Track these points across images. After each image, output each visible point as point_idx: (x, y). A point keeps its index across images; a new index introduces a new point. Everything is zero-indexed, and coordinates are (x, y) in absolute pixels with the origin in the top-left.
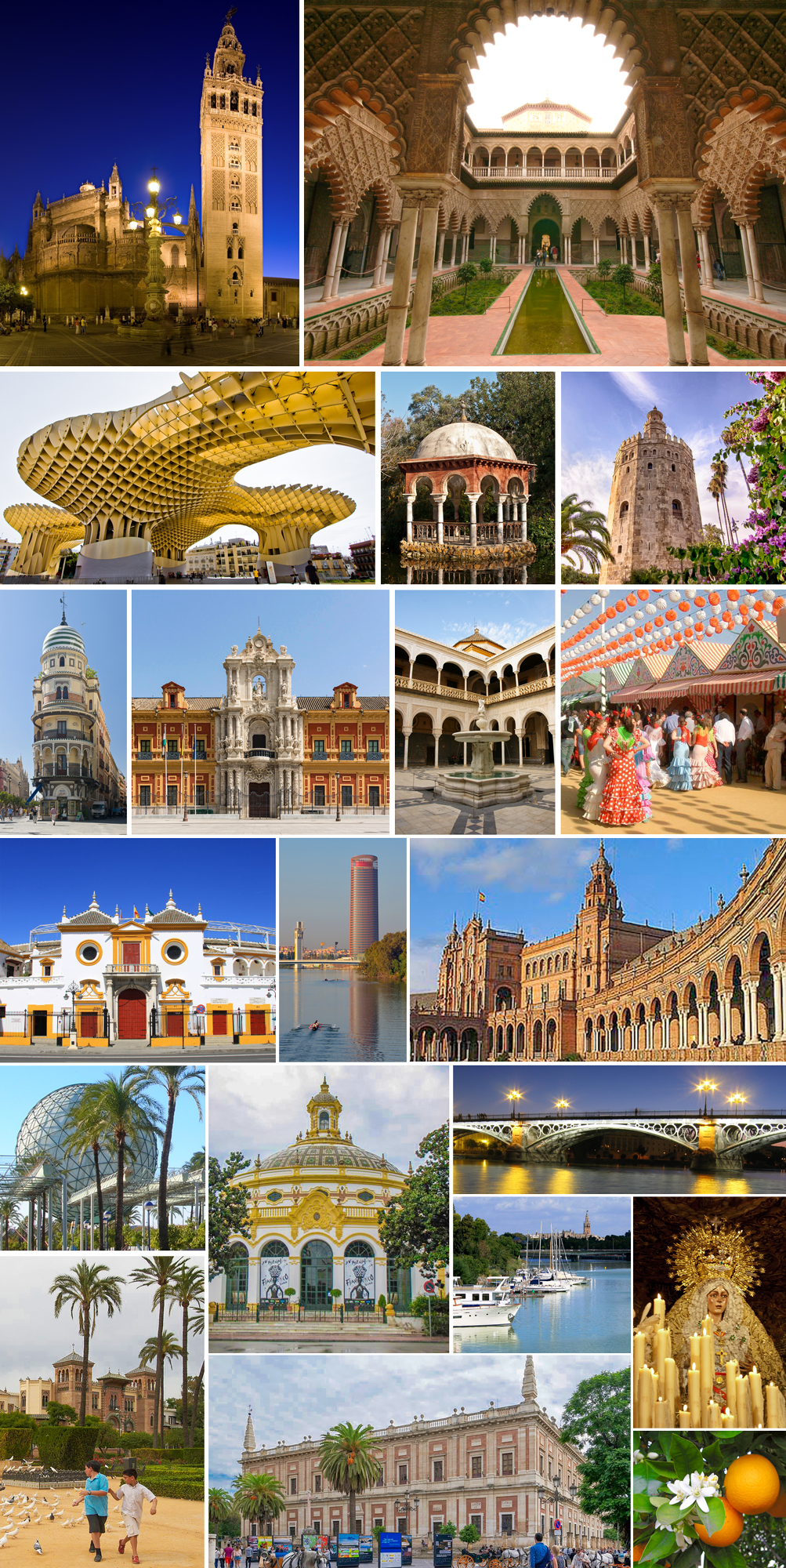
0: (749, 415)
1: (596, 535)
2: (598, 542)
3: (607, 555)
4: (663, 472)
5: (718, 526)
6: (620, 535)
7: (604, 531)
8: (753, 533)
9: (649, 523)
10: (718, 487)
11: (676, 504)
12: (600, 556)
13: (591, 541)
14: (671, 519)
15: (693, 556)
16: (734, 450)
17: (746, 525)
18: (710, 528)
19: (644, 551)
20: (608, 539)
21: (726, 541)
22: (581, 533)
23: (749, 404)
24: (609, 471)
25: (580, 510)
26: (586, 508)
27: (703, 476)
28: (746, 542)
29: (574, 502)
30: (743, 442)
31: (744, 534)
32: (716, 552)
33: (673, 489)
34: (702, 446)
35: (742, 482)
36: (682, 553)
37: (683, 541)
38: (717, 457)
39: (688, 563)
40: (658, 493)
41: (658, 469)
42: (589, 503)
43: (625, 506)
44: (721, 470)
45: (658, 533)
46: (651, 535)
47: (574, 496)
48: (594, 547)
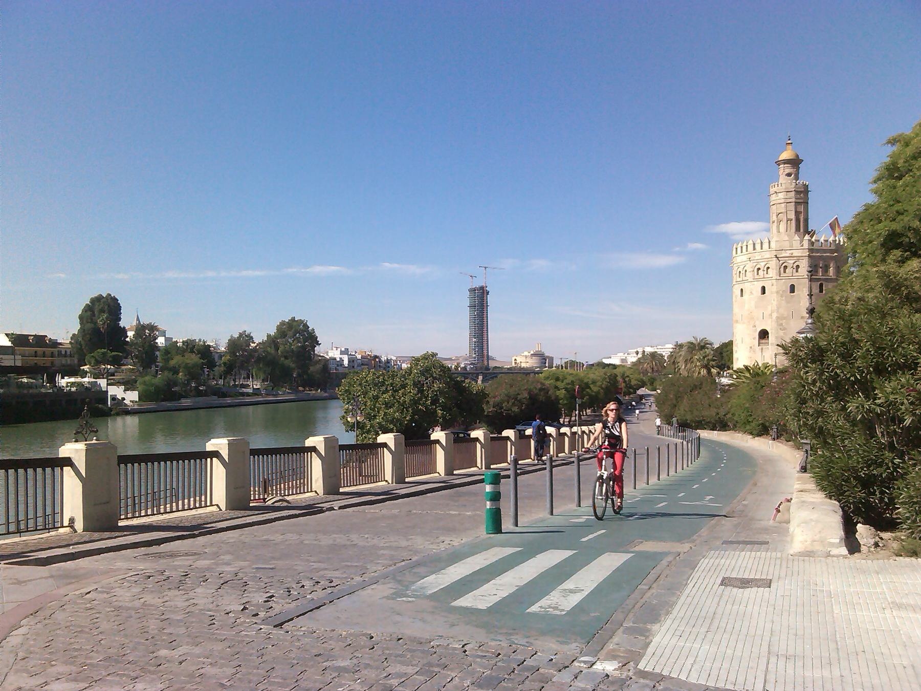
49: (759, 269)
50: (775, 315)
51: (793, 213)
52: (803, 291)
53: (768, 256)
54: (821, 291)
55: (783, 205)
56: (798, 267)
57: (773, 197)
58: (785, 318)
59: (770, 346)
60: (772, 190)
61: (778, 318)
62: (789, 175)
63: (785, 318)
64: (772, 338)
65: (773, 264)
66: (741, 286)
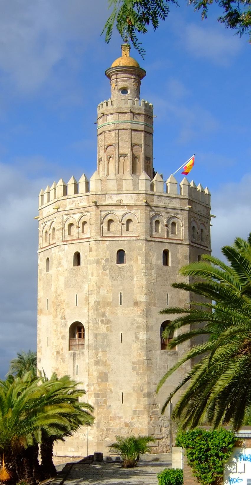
49: (71, 225)
50: (93, 299)
51: (128, 145)
52: (136, 262)
53: (84, 204)
54: (166, 262)
55: (113, 134)
56: (129, 221)
57: (100, 122)
58: (108, 304)
59: (86, 351)
60: (99, 112)
61: (97, 303)
62: (124, 91)
63: (108, 304)
65: (91, 216)
66: (47, 254)
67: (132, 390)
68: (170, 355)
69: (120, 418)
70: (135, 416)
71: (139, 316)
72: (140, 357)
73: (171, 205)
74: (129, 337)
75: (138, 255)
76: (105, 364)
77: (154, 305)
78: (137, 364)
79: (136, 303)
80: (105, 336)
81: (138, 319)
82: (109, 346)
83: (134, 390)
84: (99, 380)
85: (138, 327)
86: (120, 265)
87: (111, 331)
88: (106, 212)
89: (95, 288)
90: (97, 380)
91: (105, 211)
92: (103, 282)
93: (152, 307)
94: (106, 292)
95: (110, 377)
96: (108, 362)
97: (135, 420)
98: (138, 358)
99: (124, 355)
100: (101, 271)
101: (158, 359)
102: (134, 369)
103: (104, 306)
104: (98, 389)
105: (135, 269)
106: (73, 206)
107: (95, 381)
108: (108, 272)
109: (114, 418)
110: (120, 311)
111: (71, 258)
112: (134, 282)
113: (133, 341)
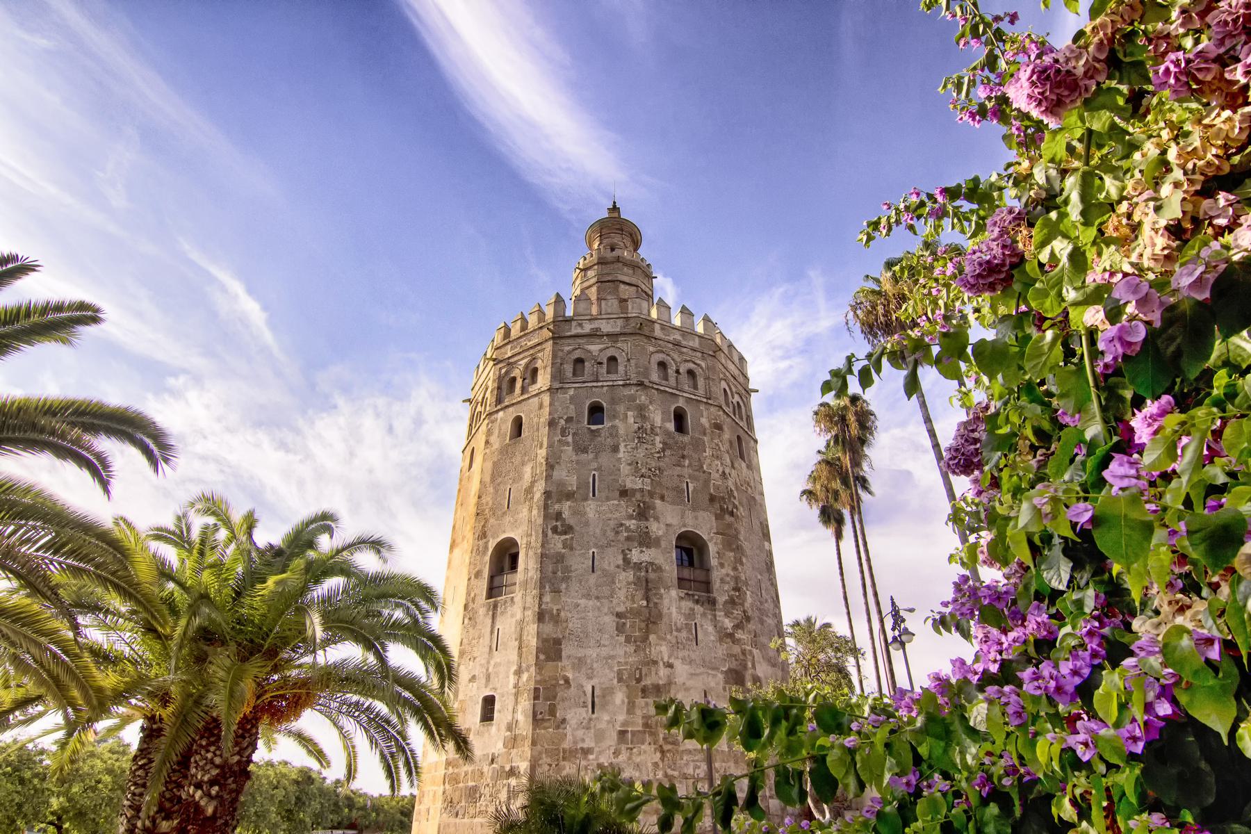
0: (950, 234)
1: (403, 657)
2: (410, 683)
3: (443, 727)
4: (642, 434)
5: (841, 628)
6: (490, 659)
7: (430, 646)
8: (967, 650)
9: (592, 616)
10: (840, 490)
11: (690, 550)
12: (416, 734)
13: (384, 680)
14: (673, 603)
15: (752, 734)
16: (897, 358)
17: (941, 623)
18: (810, 632)
19: (575, 716)
20: (446, 672)
21: (867, 679)
22: (348, 652)
23: (952, 193)
24: (449, 431)
25: (345, 570)
26: (367, 562)
27: (786, 449)
28: (942, 683)
29: (325, 543)
30: (928, 329)
31: (934, 657)
32: (833, 719)
33: (680, 496)
34: (783, 346)
35: (927, 471)
36: (710, 722)
37: (716, 681)
38: (837, 382)
39: (731, 757)
40: (623, 511)
41: (624, 423)
42: (376, 545)
43: (506, 557)
44: (849, 429)
45: (623, 653)
46: (600, 657)
47: (325, 522)
48: (394, 701)
58: (570, 496)
61: (547, 495)
64: (527, 563)
67: (615, 681)
68: (697, 602)
69: (586, 752)
70: (623, 747)
71: (630, 517)
72: (634, 602)
73: (684, 343)
74: (611, 560)
75: (628, 409)
76: (556, 619)
77: (662, 498)
78: (626, 618)
79: (624, 493)
80: (560, 559)
81: (627, 523)
82: (566, 579)
83: (620, 680)
84: (542, 657)
85: (628, 539)
86: (593, 427)
87: (572, 549)
88: (570, 348)
89: (544, 467)
90: (537, 657)
91: (569, 345)
92: (560, 457)
93: (658, 502)
94: (564, 473)
95: (568, 650)
96: (562, 614)
97: (622, 758)
98: (629, 604)
99: (597, 598)
100: (556, 439)
101: (674, 610)
102: (620, 629)
103: (559, 501)
104: (538, 678)
105: (621, 432)
106: (517, 350)
107: (532, 660)
108: (570, 439)
109: (569, 754)
110: (591, 508)
111: (508, 427)
112: (621, 455)
113: (618, 567)
